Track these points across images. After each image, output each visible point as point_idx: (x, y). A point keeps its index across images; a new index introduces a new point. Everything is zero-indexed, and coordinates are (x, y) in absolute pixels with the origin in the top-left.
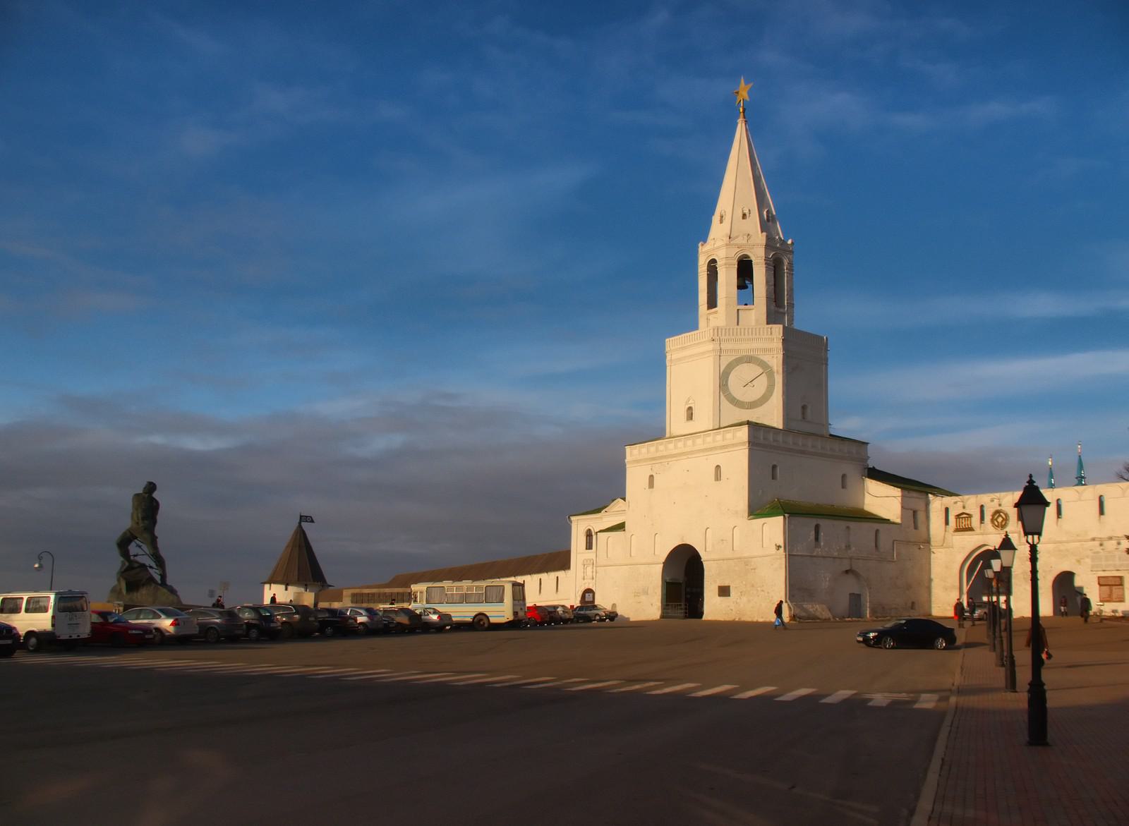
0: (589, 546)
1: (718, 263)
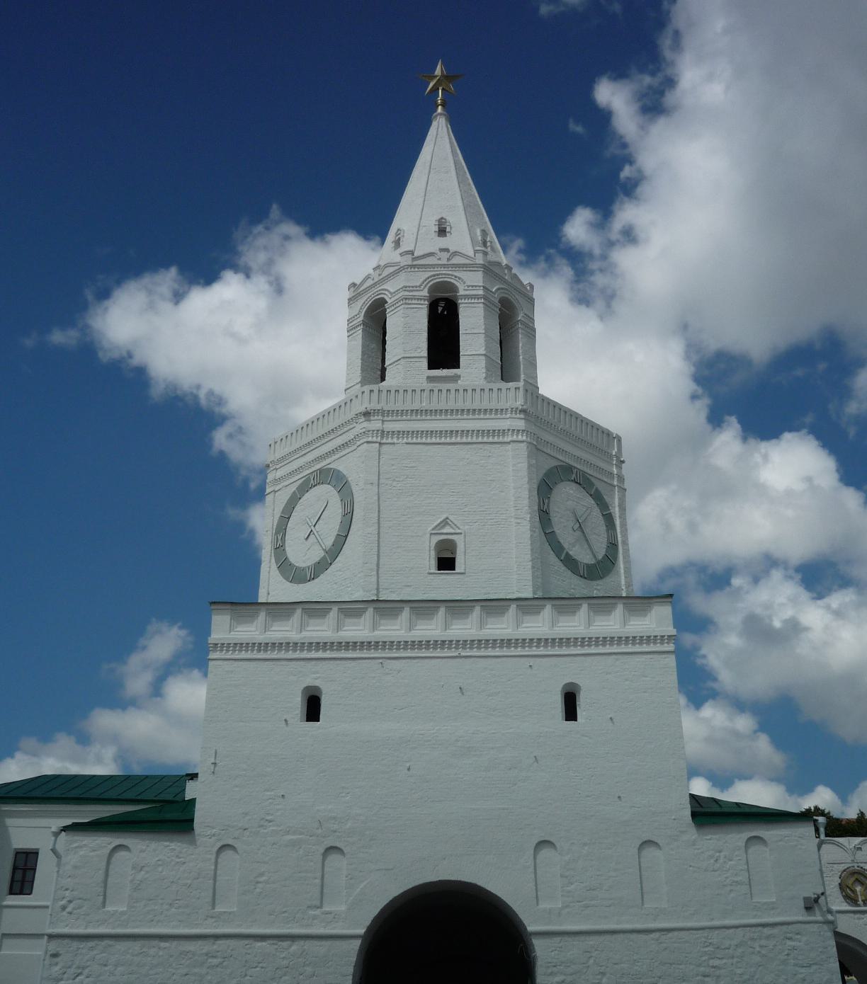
1: (461, 292)
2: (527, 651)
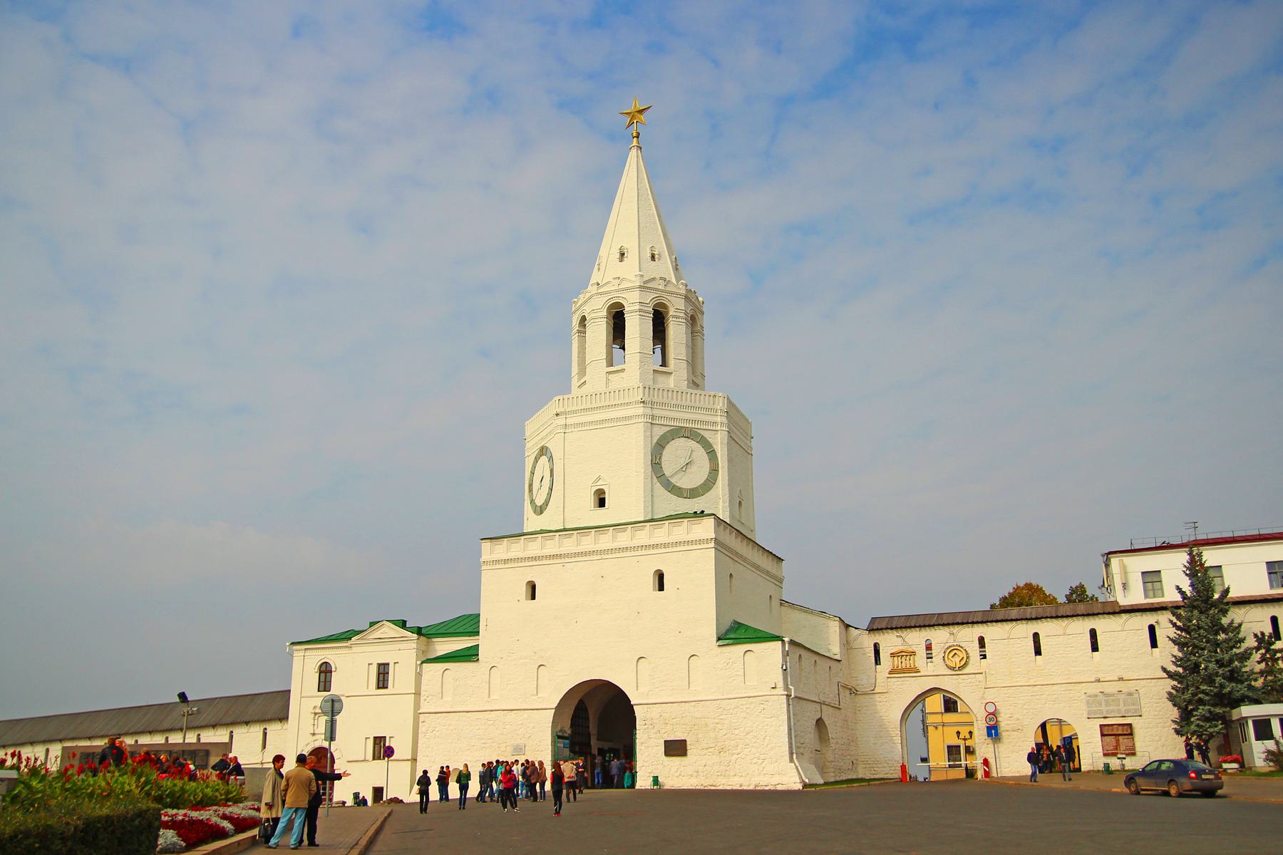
1: (627, 309)
2: (636, 553)
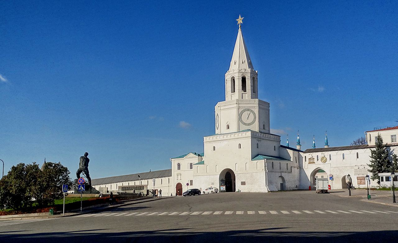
0: (179, 168)
